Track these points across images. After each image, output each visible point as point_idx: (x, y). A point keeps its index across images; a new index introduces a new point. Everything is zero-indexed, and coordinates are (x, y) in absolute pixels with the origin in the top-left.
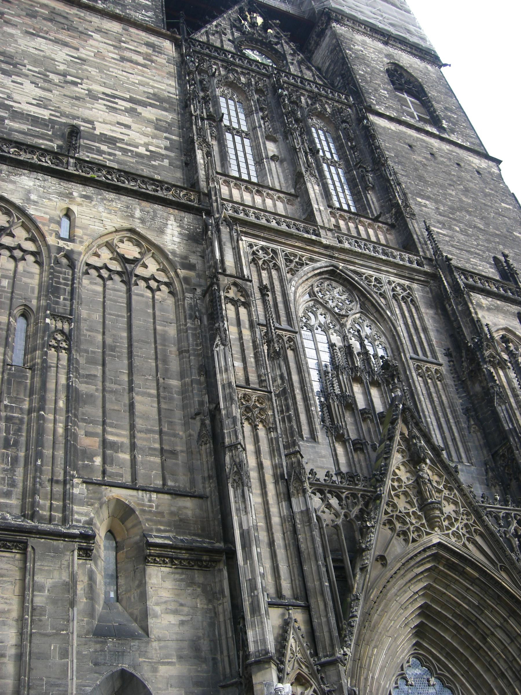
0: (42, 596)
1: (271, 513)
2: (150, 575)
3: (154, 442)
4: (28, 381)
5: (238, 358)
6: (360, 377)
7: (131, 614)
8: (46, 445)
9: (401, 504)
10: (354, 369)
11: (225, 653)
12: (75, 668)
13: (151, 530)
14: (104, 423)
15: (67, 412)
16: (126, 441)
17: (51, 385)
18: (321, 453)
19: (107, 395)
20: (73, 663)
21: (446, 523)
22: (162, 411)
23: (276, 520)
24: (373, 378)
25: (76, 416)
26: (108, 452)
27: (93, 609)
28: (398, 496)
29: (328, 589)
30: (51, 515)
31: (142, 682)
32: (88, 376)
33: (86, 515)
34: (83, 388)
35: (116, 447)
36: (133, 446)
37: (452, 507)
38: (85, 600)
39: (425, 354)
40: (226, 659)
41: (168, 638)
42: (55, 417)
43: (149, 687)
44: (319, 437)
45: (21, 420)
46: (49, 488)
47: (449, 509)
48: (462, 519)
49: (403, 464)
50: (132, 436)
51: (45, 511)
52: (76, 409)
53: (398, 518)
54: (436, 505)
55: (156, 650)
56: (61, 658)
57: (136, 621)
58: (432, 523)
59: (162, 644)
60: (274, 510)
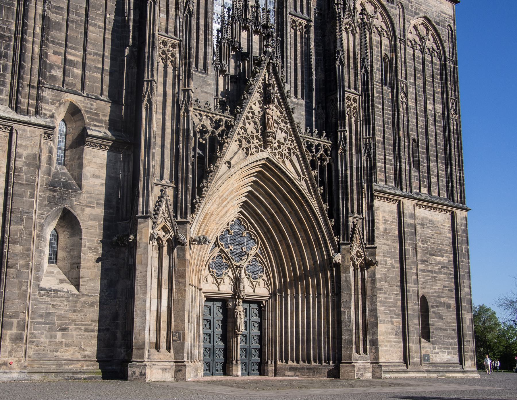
0: (21, 161)
1: (166, 127)
2: (86, 153)
3: (98, 63)
4: (15, 8)
5: (163, 11)
6: (248, 27)
7: (72, 175)
8: (26, 60)
9: (250, 128)
10: (245, 19)
11: (125, 204)
12: (37, 205)
13: (90, 125)
14: (66, 46)
15: (42, 36)
16: (80, 60)
17: (31, 15)
18: (208, 82)
19: (70, 24)
20: (36, 201)
21: (276, 145)
22: (106, 39)
23: (168, 131)
24: (257, 29)
25: (47, 39)
26: (67, 67)
27: (50, 170)
28: (249, 123)
29: (191, 180)
30: (28, 109)
31: (75, 216)
32: (58, 8)
33: (50, 111)
34: (53, 17)
35: (72, 63)
36: (84, 65)
37: (284, 135)
38: (46, 165)
39: (302, 11)
40: (125, 208)
41: (93, 192)
42: (33, 40)
43: (79, 219)
44: (209, 70)
45: (10, 38)
46: (27, 91)
47: (281, 136)
48: (287, 144)
49: (259, 102)
50: (84, 58)
51: (24, 106)
52: (48, 34)
53: (245, 138)
54: (271, 134)
55: (85, 198)
56: (30, 198)
57: (75, 179)
58: (266, 144)
59: (89, 195)
60: (168, 124)
